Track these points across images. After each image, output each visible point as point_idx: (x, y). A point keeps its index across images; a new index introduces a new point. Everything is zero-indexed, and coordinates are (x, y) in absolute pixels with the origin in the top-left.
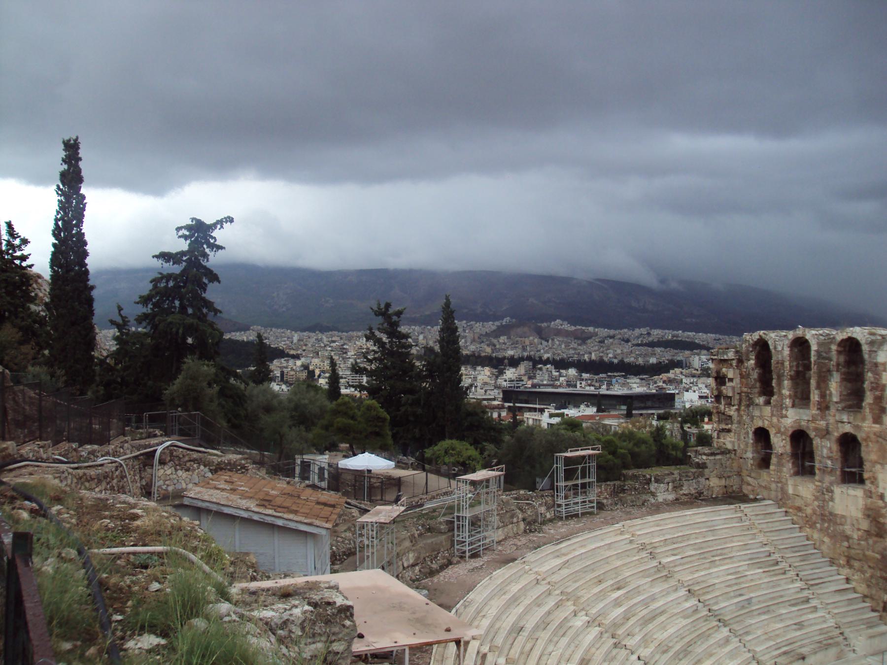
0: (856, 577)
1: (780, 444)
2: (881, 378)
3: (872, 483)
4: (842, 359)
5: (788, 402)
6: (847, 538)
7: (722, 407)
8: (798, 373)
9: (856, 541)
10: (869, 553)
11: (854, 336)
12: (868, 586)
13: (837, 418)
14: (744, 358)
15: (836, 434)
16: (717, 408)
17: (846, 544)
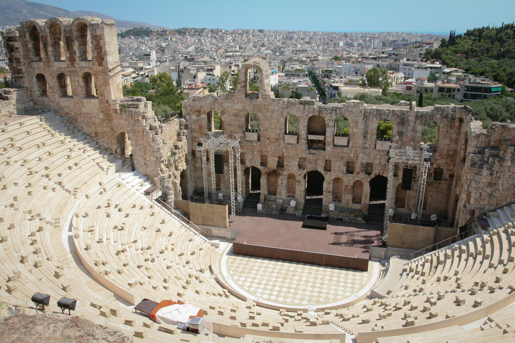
0: (100, 141)
1: (51, 82)
2: (99, 43)
3: (101, 95)
4: (78, 34)
5: (52, 58)
6: (94, 124)
7: (15, 65)
8: (55, 42)
9: (98, 125)
10: (105, 129)
11: (83, 21)
12: (107, 144)
13: (80, 66)
14: (23, 35)
15: (81, 74)
16: (11, 65)
17: (94, 127)
